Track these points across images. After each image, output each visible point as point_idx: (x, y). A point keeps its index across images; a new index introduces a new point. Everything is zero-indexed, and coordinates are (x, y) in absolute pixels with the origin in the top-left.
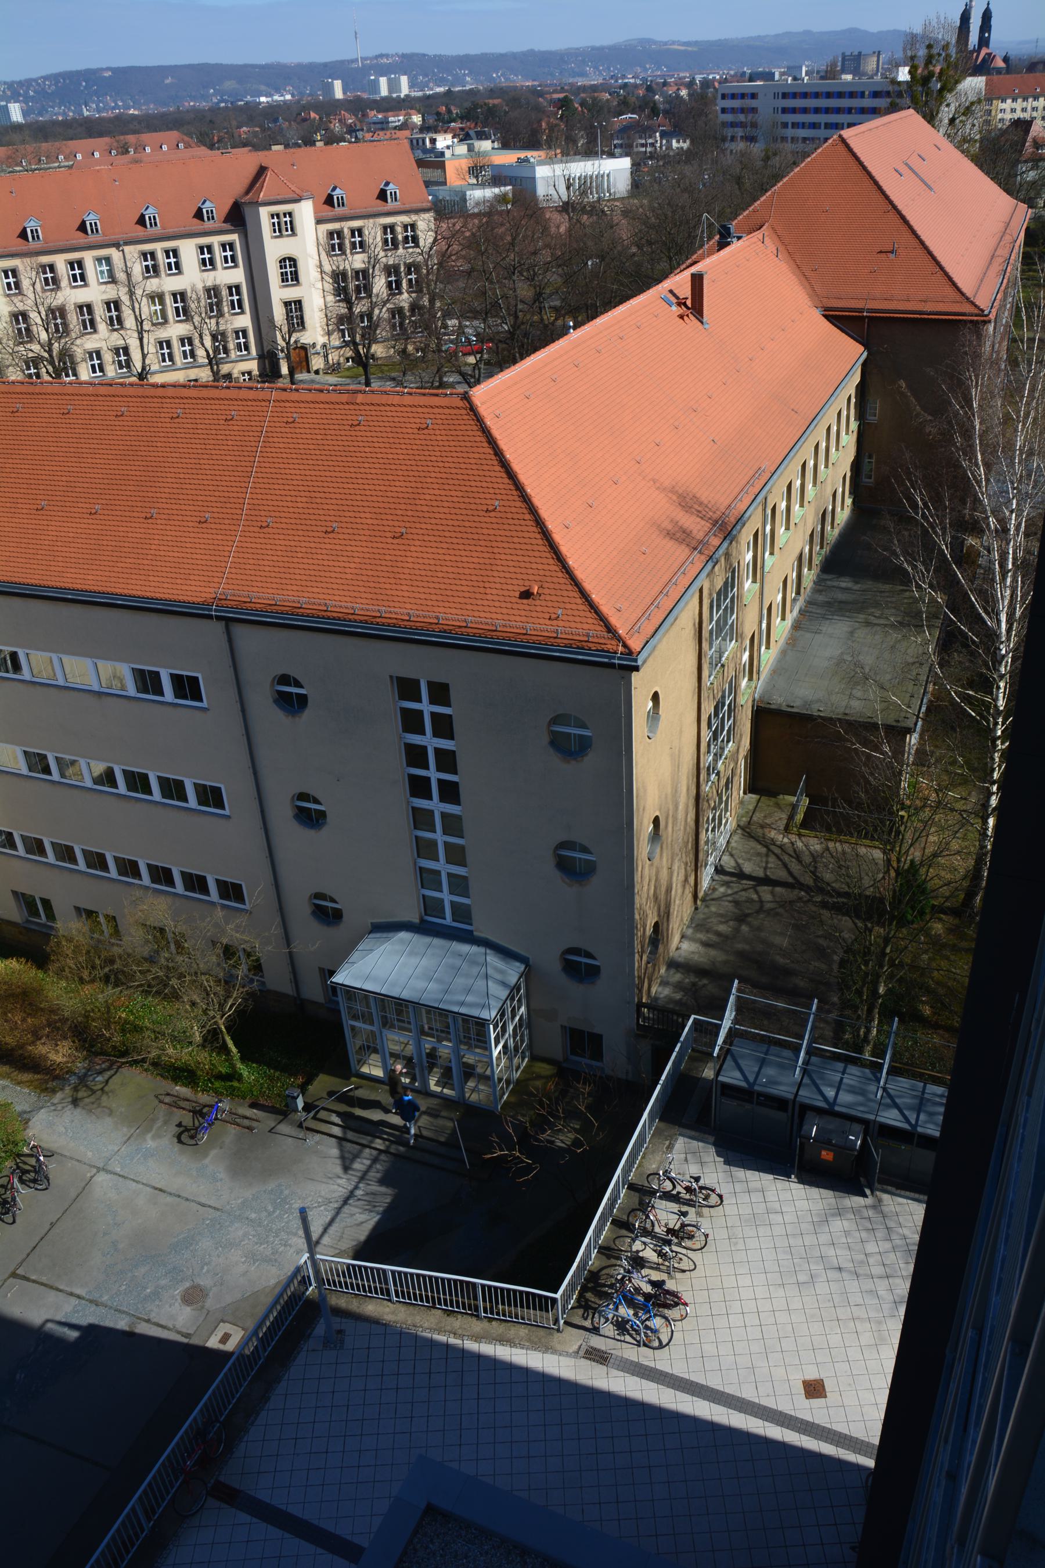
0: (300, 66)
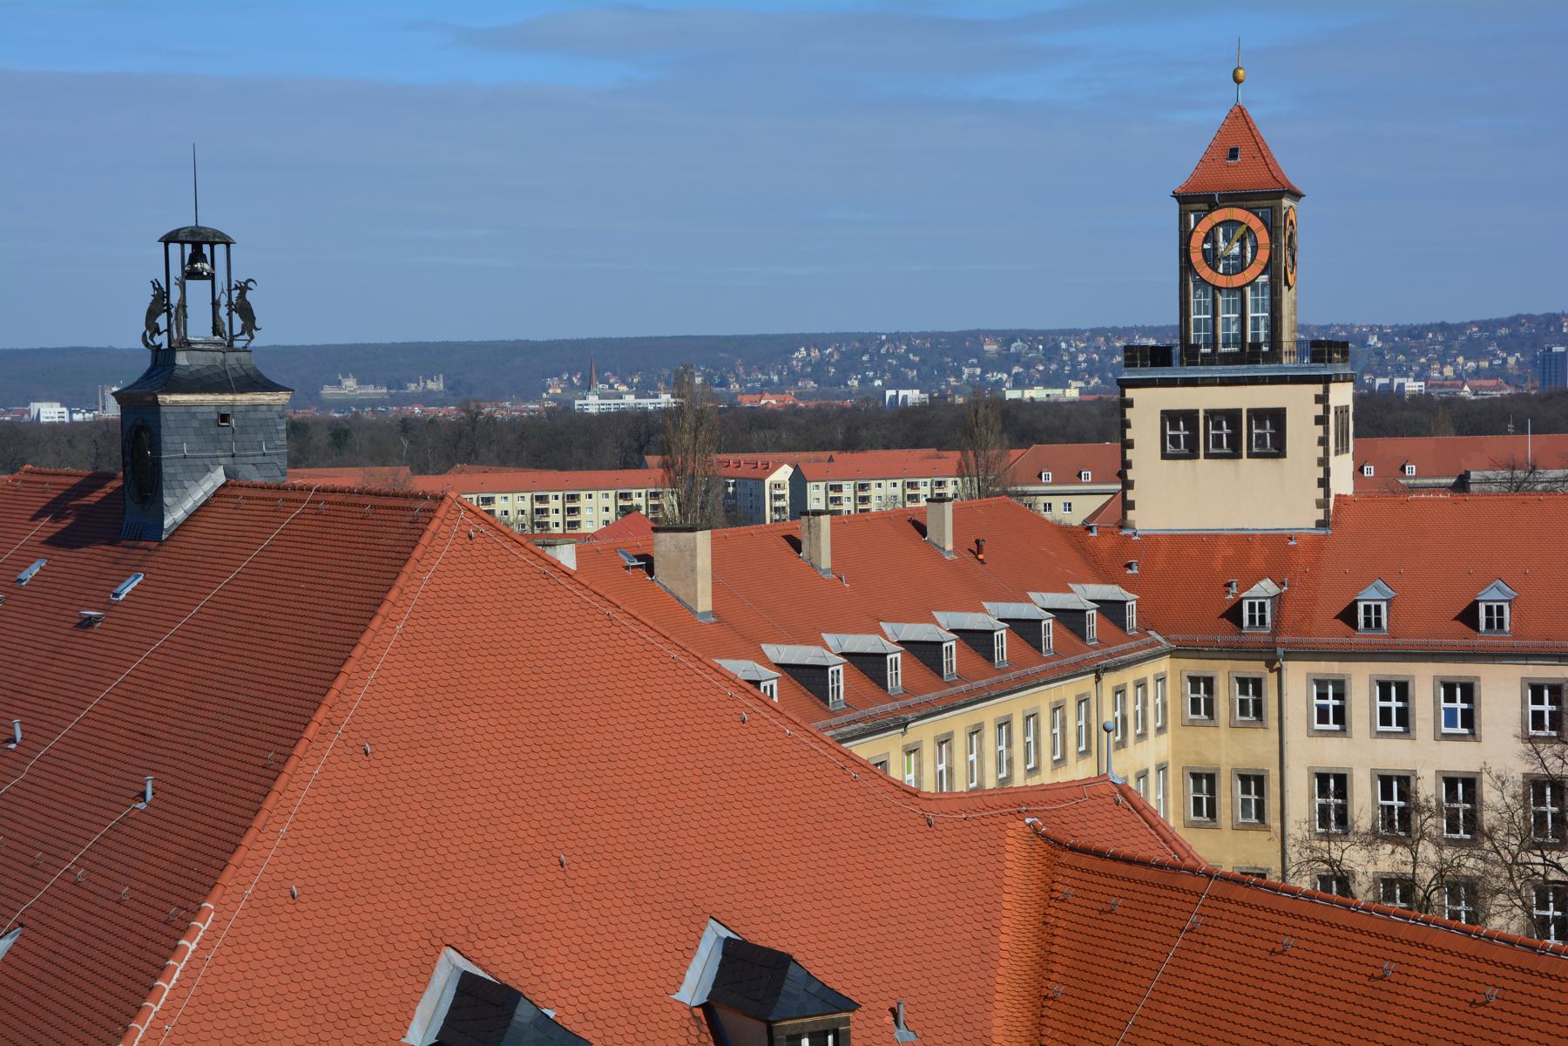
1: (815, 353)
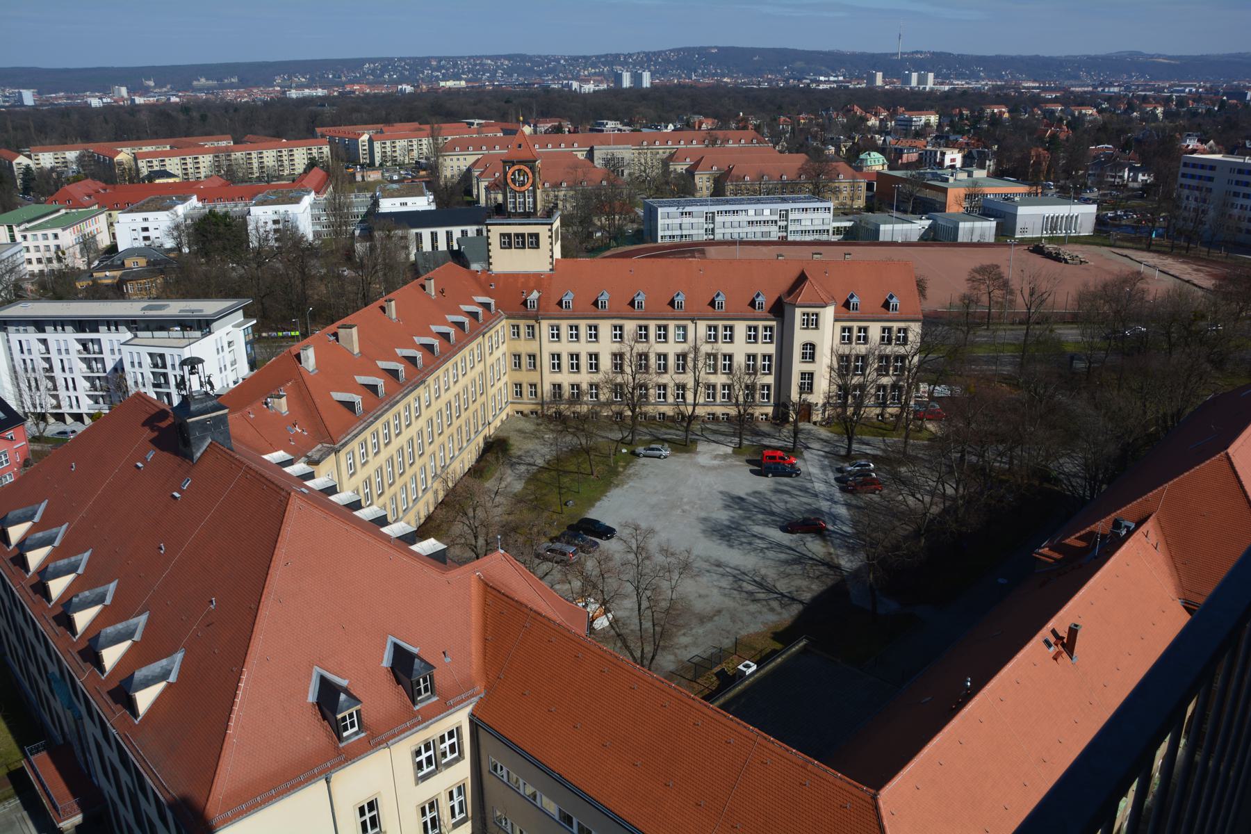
0: (854, 55)
1: (372, 66)
